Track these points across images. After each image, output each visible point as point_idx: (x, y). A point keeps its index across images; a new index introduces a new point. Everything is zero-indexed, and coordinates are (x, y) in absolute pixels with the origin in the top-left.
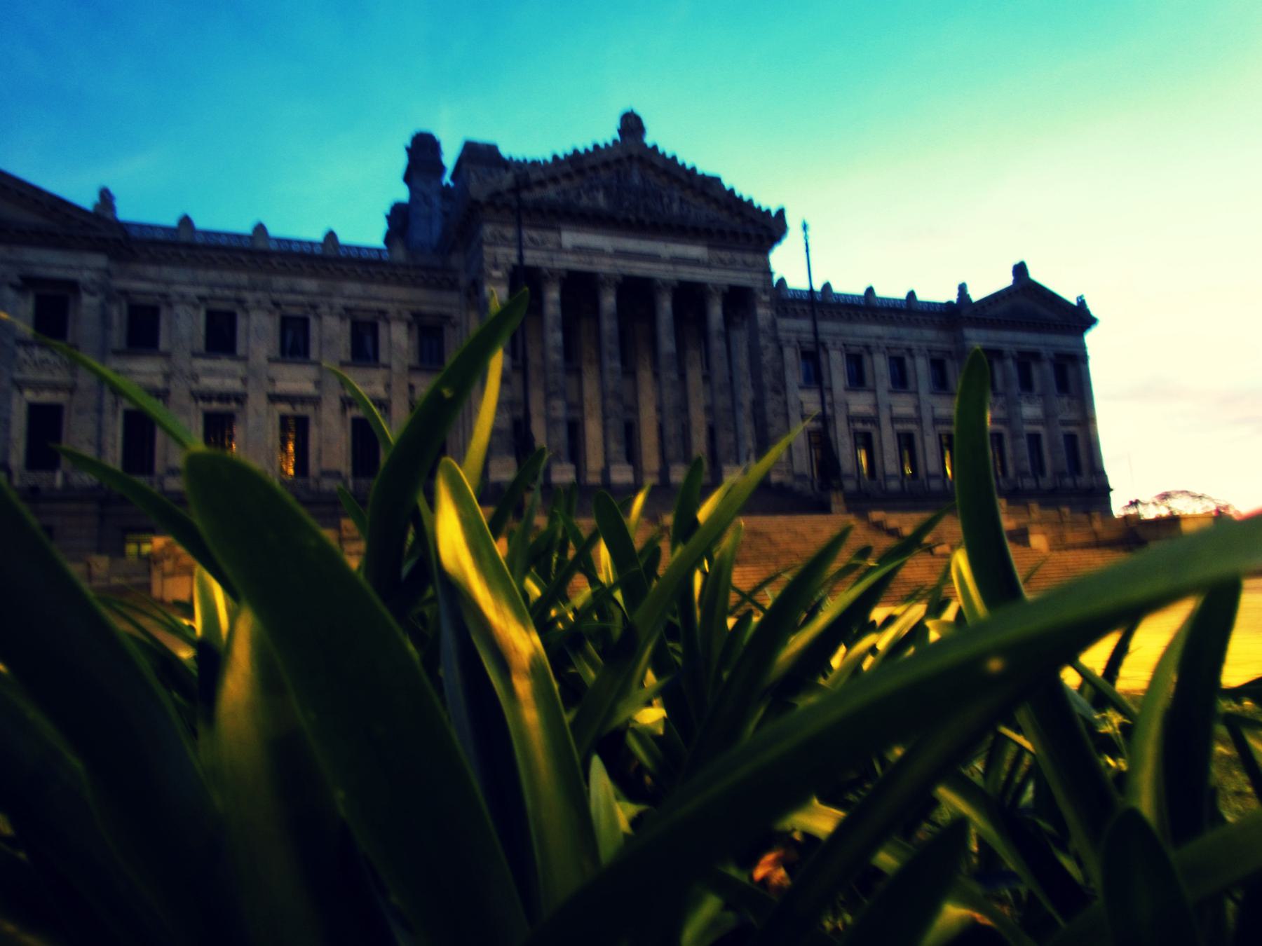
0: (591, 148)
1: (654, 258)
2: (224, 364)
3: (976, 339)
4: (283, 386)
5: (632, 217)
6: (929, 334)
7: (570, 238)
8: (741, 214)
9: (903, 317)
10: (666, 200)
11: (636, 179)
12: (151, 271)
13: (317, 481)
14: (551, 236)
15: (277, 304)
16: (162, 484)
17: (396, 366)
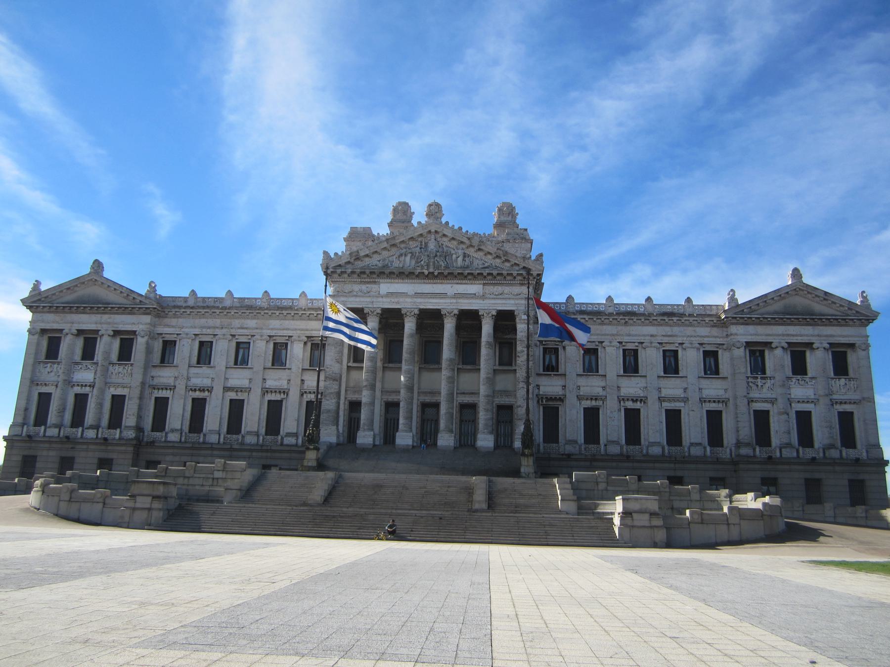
1: (443, 295)
2: (204, 370)
3: (744, 333)
4: (232, 383)
5: (426, 272)
6: (703, 331)
7: (386, 287)
9: (675, 319)
10: (454, 256)
11: (432, 246)
12: (174, 321)
13: (243, 437)
14: (374, 287)
15: (233, 336)
16: (166, 436)
17: (294, 369)
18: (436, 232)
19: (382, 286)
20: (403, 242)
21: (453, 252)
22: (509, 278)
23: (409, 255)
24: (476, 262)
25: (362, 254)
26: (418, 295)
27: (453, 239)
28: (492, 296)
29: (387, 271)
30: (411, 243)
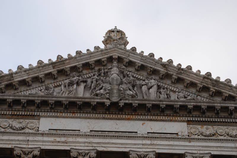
0: (74, 54)
1: (131, 135)
5: (108, 103)
8: (218, 93)
10: (144, 88)
14: (31, 123)
18: (120, 60)
19: (42, 120)
20: (74, 69)
21: (144, 83)
22: (222, 114)
23: (82, 86)
24: (174, 97)
25: (17, 79)
26: (94, 134)
27: (142, 68)
28: (199, 137)
29: (51, 100)
30: (85, 72)
